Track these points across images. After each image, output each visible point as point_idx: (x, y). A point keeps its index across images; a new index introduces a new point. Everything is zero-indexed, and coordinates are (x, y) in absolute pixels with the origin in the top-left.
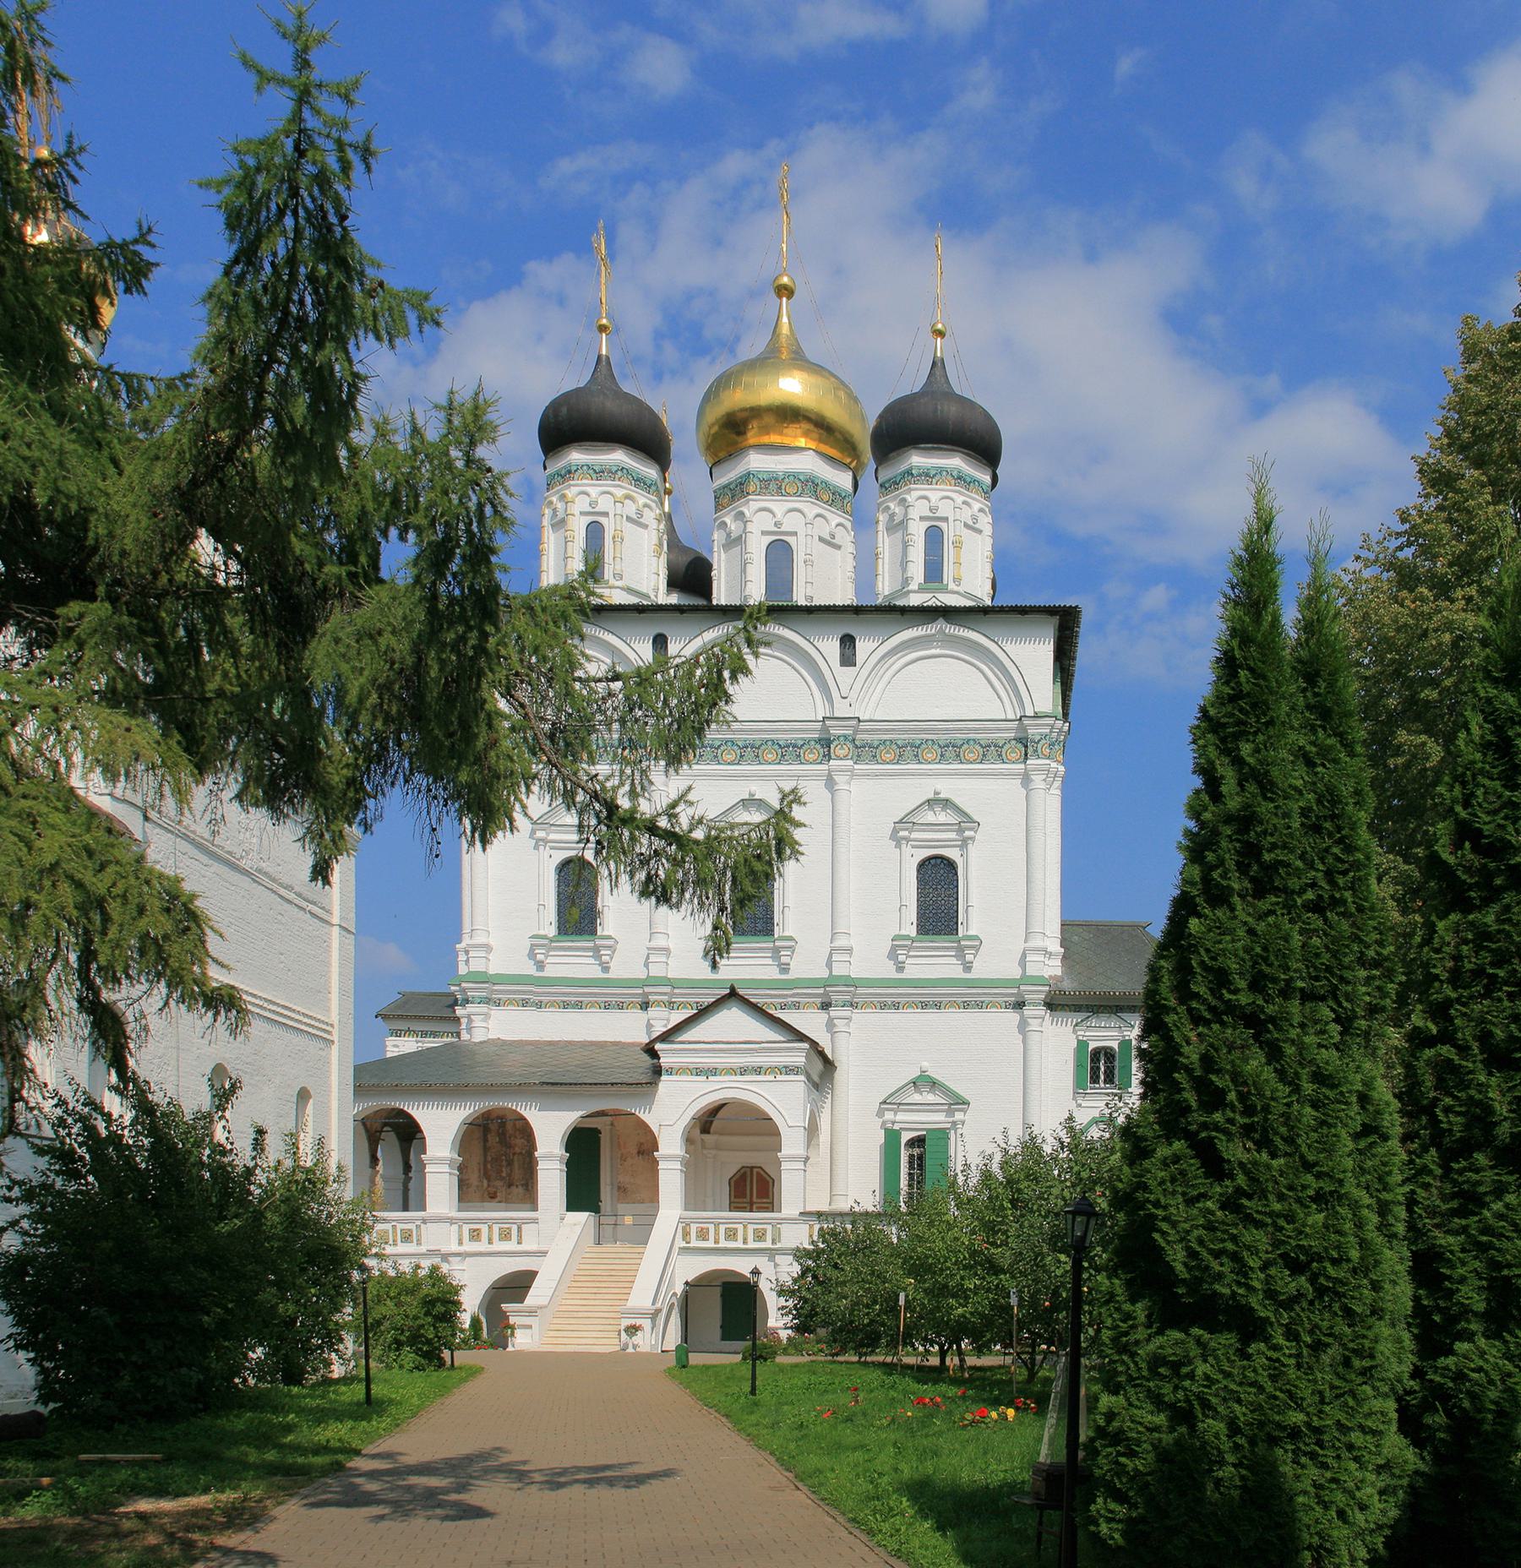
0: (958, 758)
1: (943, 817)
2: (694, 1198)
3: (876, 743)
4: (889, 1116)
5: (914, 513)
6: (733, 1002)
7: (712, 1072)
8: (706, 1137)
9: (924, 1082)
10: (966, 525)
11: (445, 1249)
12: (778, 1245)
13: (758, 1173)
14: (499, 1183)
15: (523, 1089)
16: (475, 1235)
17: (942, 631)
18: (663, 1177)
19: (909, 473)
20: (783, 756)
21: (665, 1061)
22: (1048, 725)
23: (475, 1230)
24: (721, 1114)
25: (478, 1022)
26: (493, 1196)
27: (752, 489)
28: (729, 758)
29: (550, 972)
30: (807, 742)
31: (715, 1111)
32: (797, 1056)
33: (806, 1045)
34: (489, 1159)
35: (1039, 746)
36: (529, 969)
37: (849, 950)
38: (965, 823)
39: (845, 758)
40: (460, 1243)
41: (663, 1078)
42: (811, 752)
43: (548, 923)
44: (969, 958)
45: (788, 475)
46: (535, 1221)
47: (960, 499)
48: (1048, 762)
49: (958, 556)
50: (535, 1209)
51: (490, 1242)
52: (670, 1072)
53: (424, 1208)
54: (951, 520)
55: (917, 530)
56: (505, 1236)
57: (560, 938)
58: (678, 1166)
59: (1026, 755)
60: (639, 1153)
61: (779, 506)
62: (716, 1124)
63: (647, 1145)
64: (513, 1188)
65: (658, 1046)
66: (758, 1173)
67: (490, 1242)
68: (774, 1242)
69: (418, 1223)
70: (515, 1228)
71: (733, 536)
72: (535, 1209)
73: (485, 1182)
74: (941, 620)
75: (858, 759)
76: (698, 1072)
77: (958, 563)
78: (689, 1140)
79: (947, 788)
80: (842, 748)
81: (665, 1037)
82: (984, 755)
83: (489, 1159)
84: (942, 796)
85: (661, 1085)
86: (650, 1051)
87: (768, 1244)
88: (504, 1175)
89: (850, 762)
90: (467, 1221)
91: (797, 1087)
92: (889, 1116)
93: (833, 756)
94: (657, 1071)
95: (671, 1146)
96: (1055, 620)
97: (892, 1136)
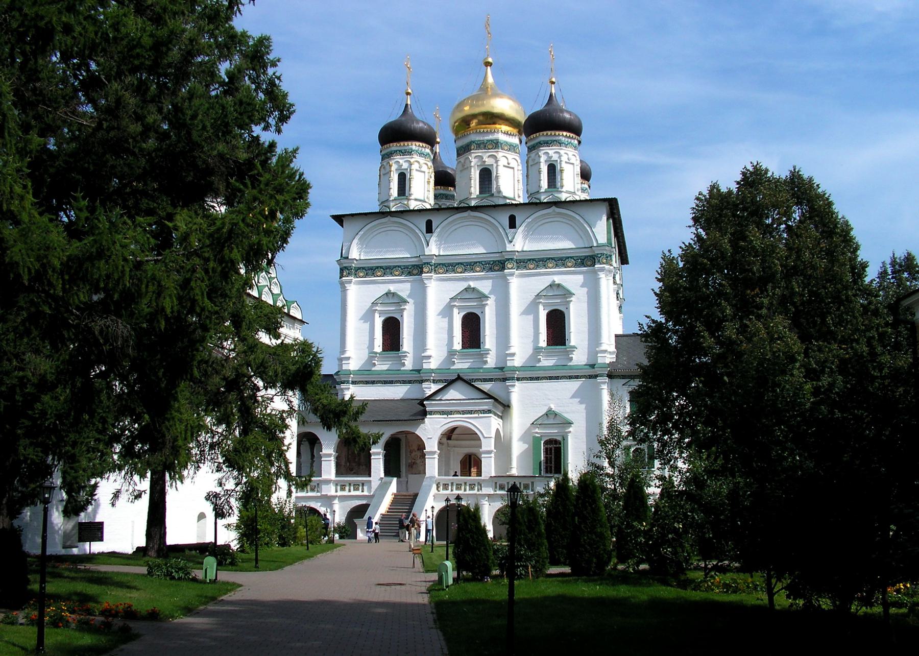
0: (564, 265)
2: (444, 468)
6: (459, 384)
7: (451, 413)
8: (449, 441)
10: (566, 162)
11: (329, 494)
13: (474, 458)
14: (354, 464)
17: (554, 211)
19: (540, 143)
24: (456, 432)
26: (351, 470)
27: (472, 147)
28: (460, 270)
31: (454, 429)
34: (350, 453)
38: (566, 294)
39: (512, 268)
40: (336, 491)
41: (428, 416)
42: (497, 266)
49: (561, 176)
50: (370, 476)
51: (350, 491)
52: (431, 413)
56: (356, 489)
59: (595, 262)
60: (418, 449)
62: (454, 436)
63: (421, 446)
64: (361, 467)
65: (425, 403)
66: (474, 458)
72: (370, 476)
73: (348, 464)
74: (554, 207)
75: (518, 268)
77: (562, 179)
78: (440, 443)
79: (558, 279)
83: (350, 453)
84: (556, 282)
86: (421, 403)
88: (357, 460)
94: (424, 413)
95: (432, 445)
96: (607, 204)
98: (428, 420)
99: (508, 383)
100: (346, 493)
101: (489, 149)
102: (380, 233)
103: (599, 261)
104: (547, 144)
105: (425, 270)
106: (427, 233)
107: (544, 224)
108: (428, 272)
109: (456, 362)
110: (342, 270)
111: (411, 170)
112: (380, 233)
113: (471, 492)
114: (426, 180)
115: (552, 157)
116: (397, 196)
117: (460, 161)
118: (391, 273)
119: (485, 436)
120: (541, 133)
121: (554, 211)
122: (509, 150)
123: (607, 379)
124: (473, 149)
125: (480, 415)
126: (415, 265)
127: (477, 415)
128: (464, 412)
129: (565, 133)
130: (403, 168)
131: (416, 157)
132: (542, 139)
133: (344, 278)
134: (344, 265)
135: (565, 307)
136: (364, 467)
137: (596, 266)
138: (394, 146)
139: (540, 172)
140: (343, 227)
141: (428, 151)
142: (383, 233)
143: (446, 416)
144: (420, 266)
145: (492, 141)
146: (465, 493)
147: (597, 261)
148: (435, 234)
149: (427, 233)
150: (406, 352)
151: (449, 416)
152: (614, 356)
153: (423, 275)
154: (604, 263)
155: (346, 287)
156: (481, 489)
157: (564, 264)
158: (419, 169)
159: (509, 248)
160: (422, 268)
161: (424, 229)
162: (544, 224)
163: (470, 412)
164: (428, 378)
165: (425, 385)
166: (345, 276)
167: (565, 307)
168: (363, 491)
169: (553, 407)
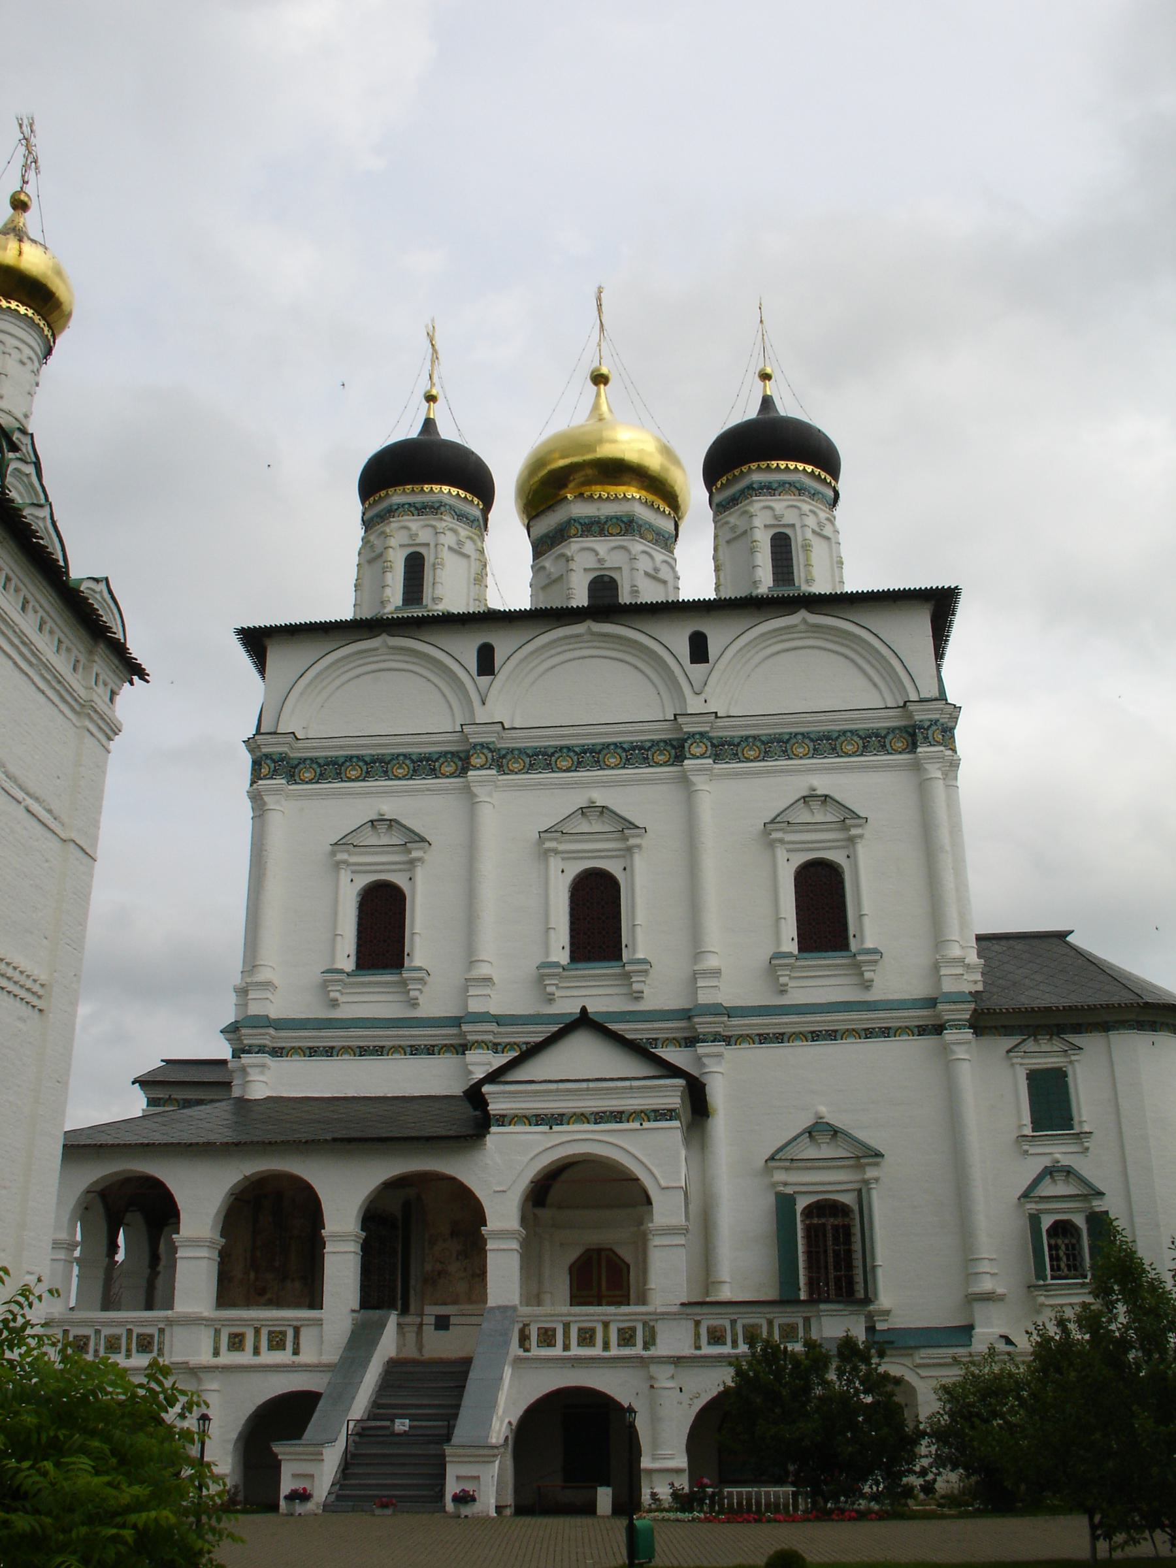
1: (820, 815)
3: (736, 741)
4: (780, 1176)
5: (758, 522)
9: (819, 1130)
11: (194, 1361)
12: (652, 1352)
15: (307, 1146)
16: (237, 1342)
18: (492, 1261)
19: (750, 487)
20: (628, 760)
21: (494, 1107)
22: (937, 710)
23: (236, 1335)
25: (254, 1075)
26: (262, 1292)
29: (345, 1012)
30: (654, 743)
32: (671, 1094)
33: (680, 1082)
35: (930, 732)
36: (321, 1012)
37: (716, 973)
39: (702, 756)
40: (216, 1353)
41: (493, 1129)
42: (661, 754)
43: (345, 954)
44: (867, 975)
45: (609, 518)
46: (319, 1323)
47: (806, 508)
48: (942, 748)
51: (256, 1351)
52: (502, 1120)
53: (170, 1307)
54: (798, 526)
55: (763, 539)
57: (359, 972)
58: (515, 1245)
61: (602, 545)
67: (256, 1351)
68: (646, 1347)
69: (161, 1326)
70: (290, 1334)
71: (554, 577)
73: (252, 1275)
75: (717, 758)
76: (539, 1119)
77: (808, 565)
79: (823, 783)
80: (698, 746)
81: (494, 1077)
82: (864, 747)
84: (819, 792)
85: (489, 1139)
87: (638, 1350)
88: (277, 1264)
89: (710, 761)
90: (230, 1322)
91: (672, 1133)
92: (780, 1176)
93: (688, 755)
97: (785, 1203)
98: (496, 1137)
99: (702, 1049)
100: (245, 1358)
101: (612, 535)
102: (358, 676)
103: (926, 738)
104: (769, 489)
105: (475, 761)
106: (479, 674)
107: (778, 653)
108: (482, 767)
109: (558, 993)
110: (257, 764)
111: (436, 545)
112: (358, 676)
113: (627, 1351)
114: (473, 576)
115: (782, 516)
116: (400, 603)
117: (543, 568)
118: (386, 772)
119: (663, 1183)
120: (754, 466)
121: (804, 621)
122: (656, 543)
123: (968, 1034)
124: (575, 536)
125: (646, 1125)
126: (446, 753)
127: (636, 1125)
128: (600, 1117)
129: (809, 468)
130: (418, 541)
131: (448, 521)
132: (757, 477)
133: (260, 782)
134: (265, 750)
135: (844, 853)
136: (297, 1284)
137: (919, 750)
138: (398, 496)
139: (752, 551)
140: (264, 678)
141: (478, 513)
142: (372, 675)
143: (546, 1128)
144: (462, 755)
145: (617, 519)
146: (606, 1354)
147: (920, 737)
148: (501, 677)
149: (479, 674)
150: (420, 969)
151: (555, 1128)
152: (979, 977)
153: (470, 773)
154: (939, 744)
155: (264, 804)
156: (654, 1344)
157: (834, 749)
158: (456, 547)
159: (694, 705)
160: (468, 757)
161: (473, 666)
162: (778, 653)
163: (618, 1116)
164: (479, 1038)
165: (472, 1056)
166: (265, 778)
167: (844, 853)
168: (296, 1352)
169: (823, 1110)
